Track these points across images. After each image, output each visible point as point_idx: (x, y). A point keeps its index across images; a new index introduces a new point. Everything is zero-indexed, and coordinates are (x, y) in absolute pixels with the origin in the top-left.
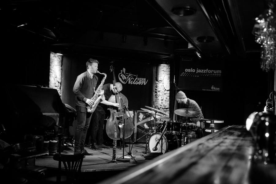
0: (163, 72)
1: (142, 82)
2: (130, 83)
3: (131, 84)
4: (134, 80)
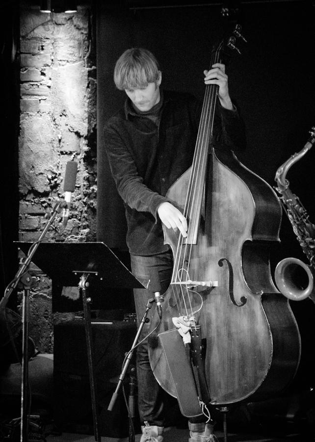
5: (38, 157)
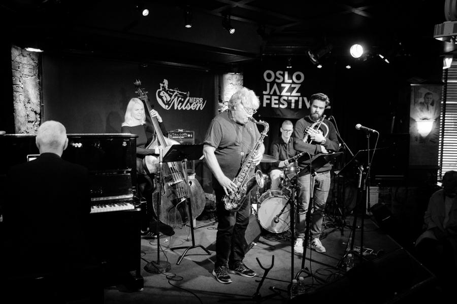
0: (230, 85)
1: (197, 104)
2: (177, 108)
3: (179, 109)
4: (184, 101)
5: (21, 124)
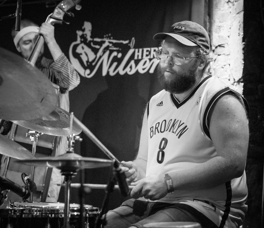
2: (108, 72)
3: (112, 74)
